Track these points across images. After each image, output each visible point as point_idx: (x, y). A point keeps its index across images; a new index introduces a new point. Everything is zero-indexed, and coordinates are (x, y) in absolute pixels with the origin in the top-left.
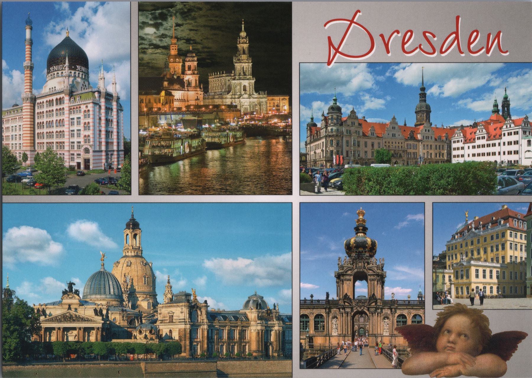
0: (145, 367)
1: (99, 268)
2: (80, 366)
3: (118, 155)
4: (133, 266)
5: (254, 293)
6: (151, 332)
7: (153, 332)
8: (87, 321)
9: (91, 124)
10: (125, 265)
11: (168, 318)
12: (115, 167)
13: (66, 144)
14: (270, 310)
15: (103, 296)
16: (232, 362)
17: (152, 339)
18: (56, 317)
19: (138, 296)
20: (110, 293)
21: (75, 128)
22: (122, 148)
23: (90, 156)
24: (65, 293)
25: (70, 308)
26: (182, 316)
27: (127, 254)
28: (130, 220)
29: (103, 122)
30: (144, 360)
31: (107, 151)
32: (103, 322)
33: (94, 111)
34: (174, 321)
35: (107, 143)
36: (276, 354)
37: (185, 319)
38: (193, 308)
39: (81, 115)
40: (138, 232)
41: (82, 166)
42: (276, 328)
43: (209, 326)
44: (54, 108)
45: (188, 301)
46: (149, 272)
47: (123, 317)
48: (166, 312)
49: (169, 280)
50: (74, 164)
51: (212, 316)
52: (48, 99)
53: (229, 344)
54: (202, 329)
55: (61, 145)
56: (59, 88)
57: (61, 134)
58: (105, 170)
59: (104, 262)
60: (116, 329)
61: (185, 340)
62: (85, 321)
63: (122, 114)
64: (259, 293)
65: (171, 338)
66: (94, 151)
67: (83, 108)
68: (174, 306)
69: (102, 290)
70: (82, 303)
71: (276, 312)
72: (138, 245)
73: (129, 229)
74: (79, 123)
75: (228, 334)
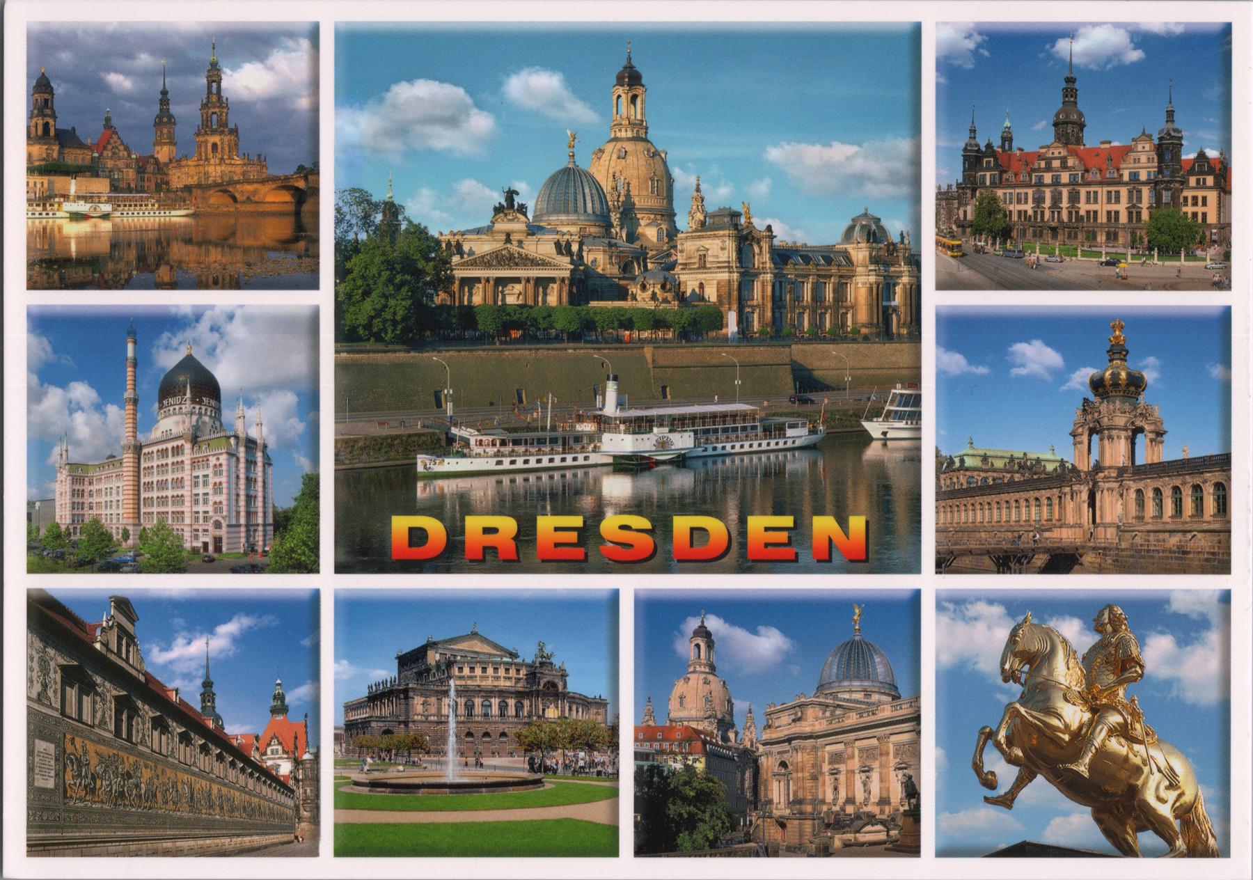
0: (653, 356)
1: (564, 163)
2: (528, 353)
3: (265, 531)
4: (630, 159)
5: (862, 212)
6: (663, 287)
9: (224, 485)
10: (615, 156)
11: (696, 260)
12: (260, 550)
13: (187, 515)
14: (894, 244)
15: (573, 217)
17: (665, 301)
18: (483, 257)
21: (201, 490)
22: (271, 521)
23: (223, 532)
24: (498, 210)
25: (508, 240)
26: (723, 257)
27: (618, 135)
28: (625, 68)
29: (242, 482)
31: (247, 526)
33: (229, 465)
35: (248, 514)
36: (904, 331)
38: (745, 240)
39: (210, 472)
40: (639, 91)
41: (211, 548)
42: (905, 280)
43: (775, 276)
44: (170, 460)
45: (736, 226)
47: (611, 257)
49: (698, 185)
50: (199, 544)
51: (782, 256)
52: (160, 447)
53: (814, 311)
54: (763, 282)
55: (179, 515)
56: (176, 430)
57: (179, 499)
58: (245, 554)
60: (598, 281)
61: (730, 303)
63: (270, 470)
64: (874, 212)
65: (702, 298)
66: (229, 526)
67: (213, 461)
70: (533, 230)
71: (905, 249)
72: (639, 117)
74: (205, 484)
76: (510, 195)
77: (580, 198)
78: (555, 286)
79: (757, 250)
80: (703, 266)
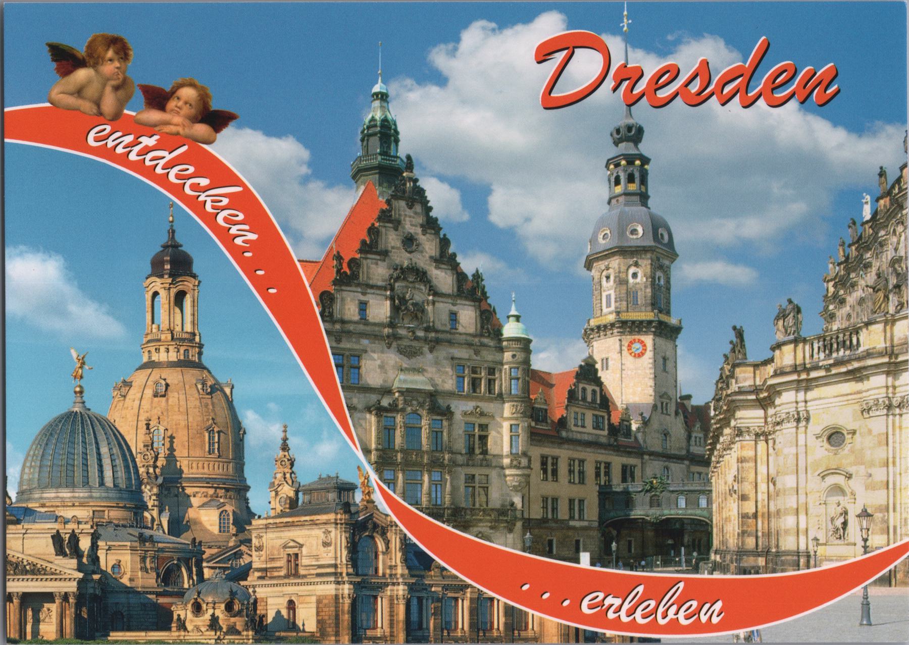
4: (173, 397)
6: (229, 607)
7: (236, 608)
8: (33, 572)
10: (149, 392)
11: (282, 563)
15: (81, 493)
17: (232, 630)
19: (189, 491)
20: (102, 484)
26: (327, 556)
27: (155, 357)
28: (165, 247)
32: (81, 575)
34: (302, 571)
37: (335, 566)
40: (188, 284)
43: (411, 588)
45: (347, 507)
46: (222, 414)
47: (143, 559)
48: (279, 542)
49: (285, 440)
54: (391, 599)
59: (82, 382)
60: (122, 599)
61: (337, 634)
62: (26, 572)
65: (292, 626)
68: (302, 525)
72: (188, 328)
73: (161, 276)
75: (474, 612)
77: (93, 461)
78: (54, 607)
79: (381, 546)
80: (293, 571)
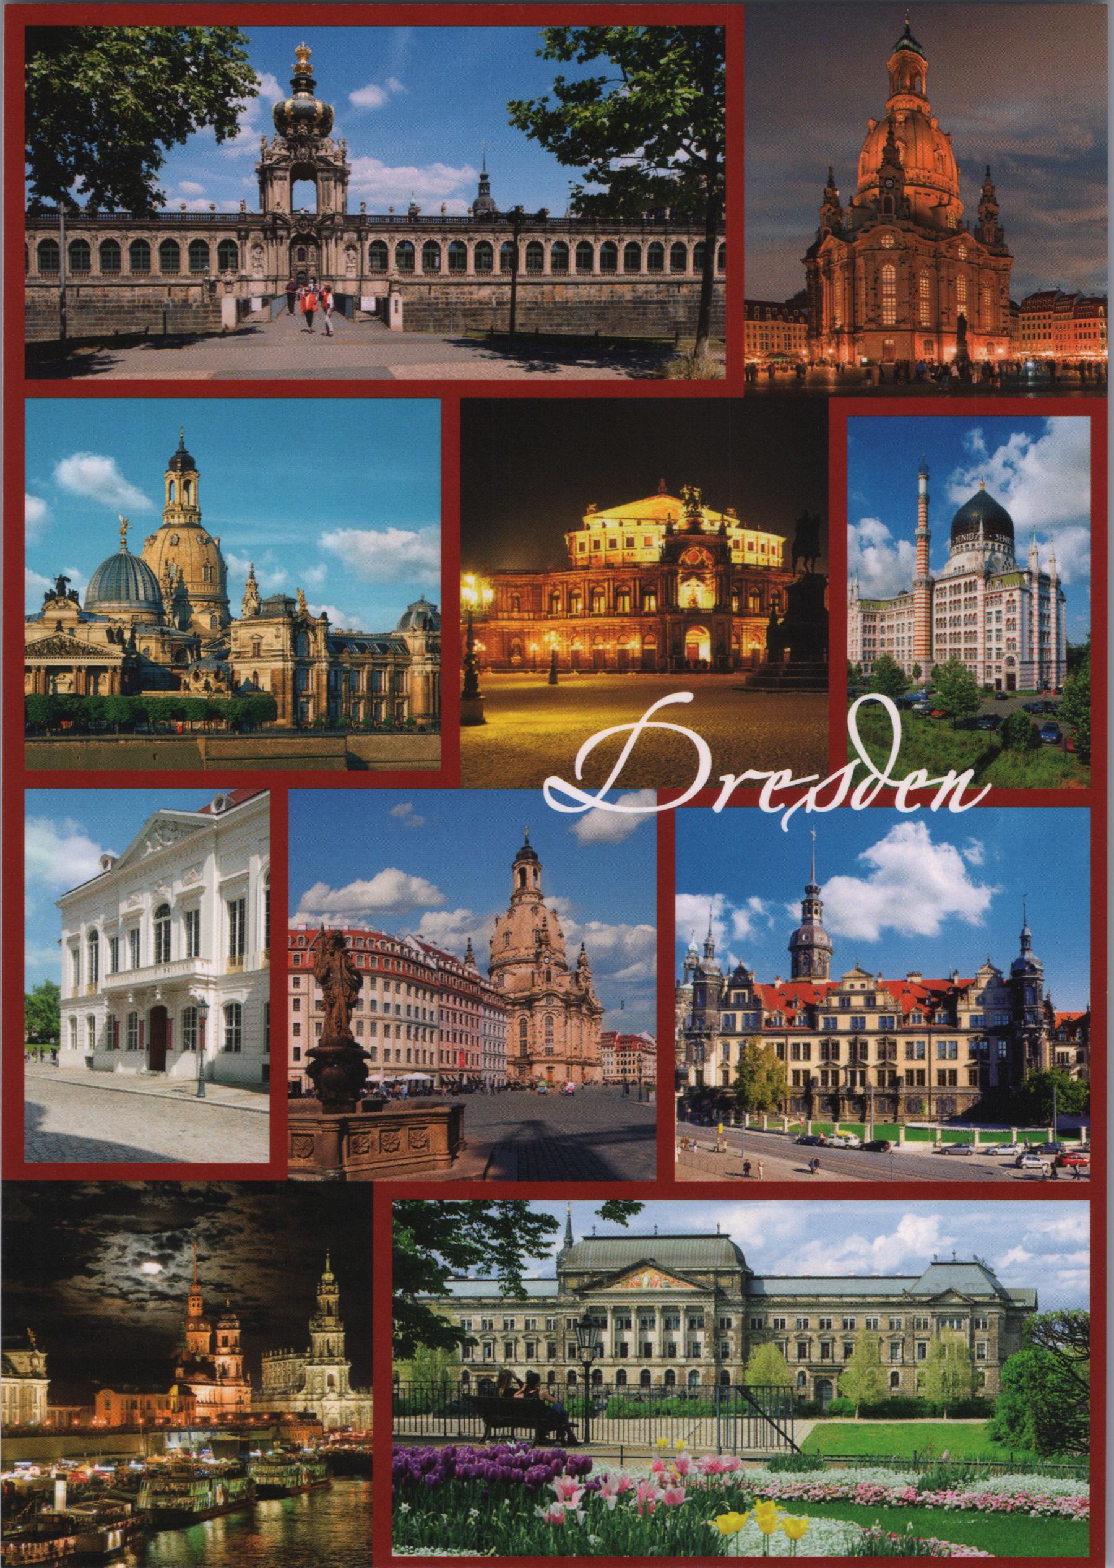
0: (207, 747)
1: (116, 549)
2: (79, 744)
4: (182, 545)
6: (216, 676)
10: (167, 543)
11: (250, 649)
15: (125, 605)
16: (375, 738)
17: (219, 690)
24: (49, 597)
25: (59, 628)
26: (278, 645)
27: (171, 521)
30: (203, 732)
40: (192, 476)
43: (331, 664)
45: (290, 614)
47: (163, 645)
51: (338, 644)
53: (369, 700)
65: (255, 688)
69: (123, 591)
70: (85, 618)
72: (192, 503)
75: (369, 679)
76: (62, 581)
78: (107, 675)
79: (312, 638)
80: (257, 654)
